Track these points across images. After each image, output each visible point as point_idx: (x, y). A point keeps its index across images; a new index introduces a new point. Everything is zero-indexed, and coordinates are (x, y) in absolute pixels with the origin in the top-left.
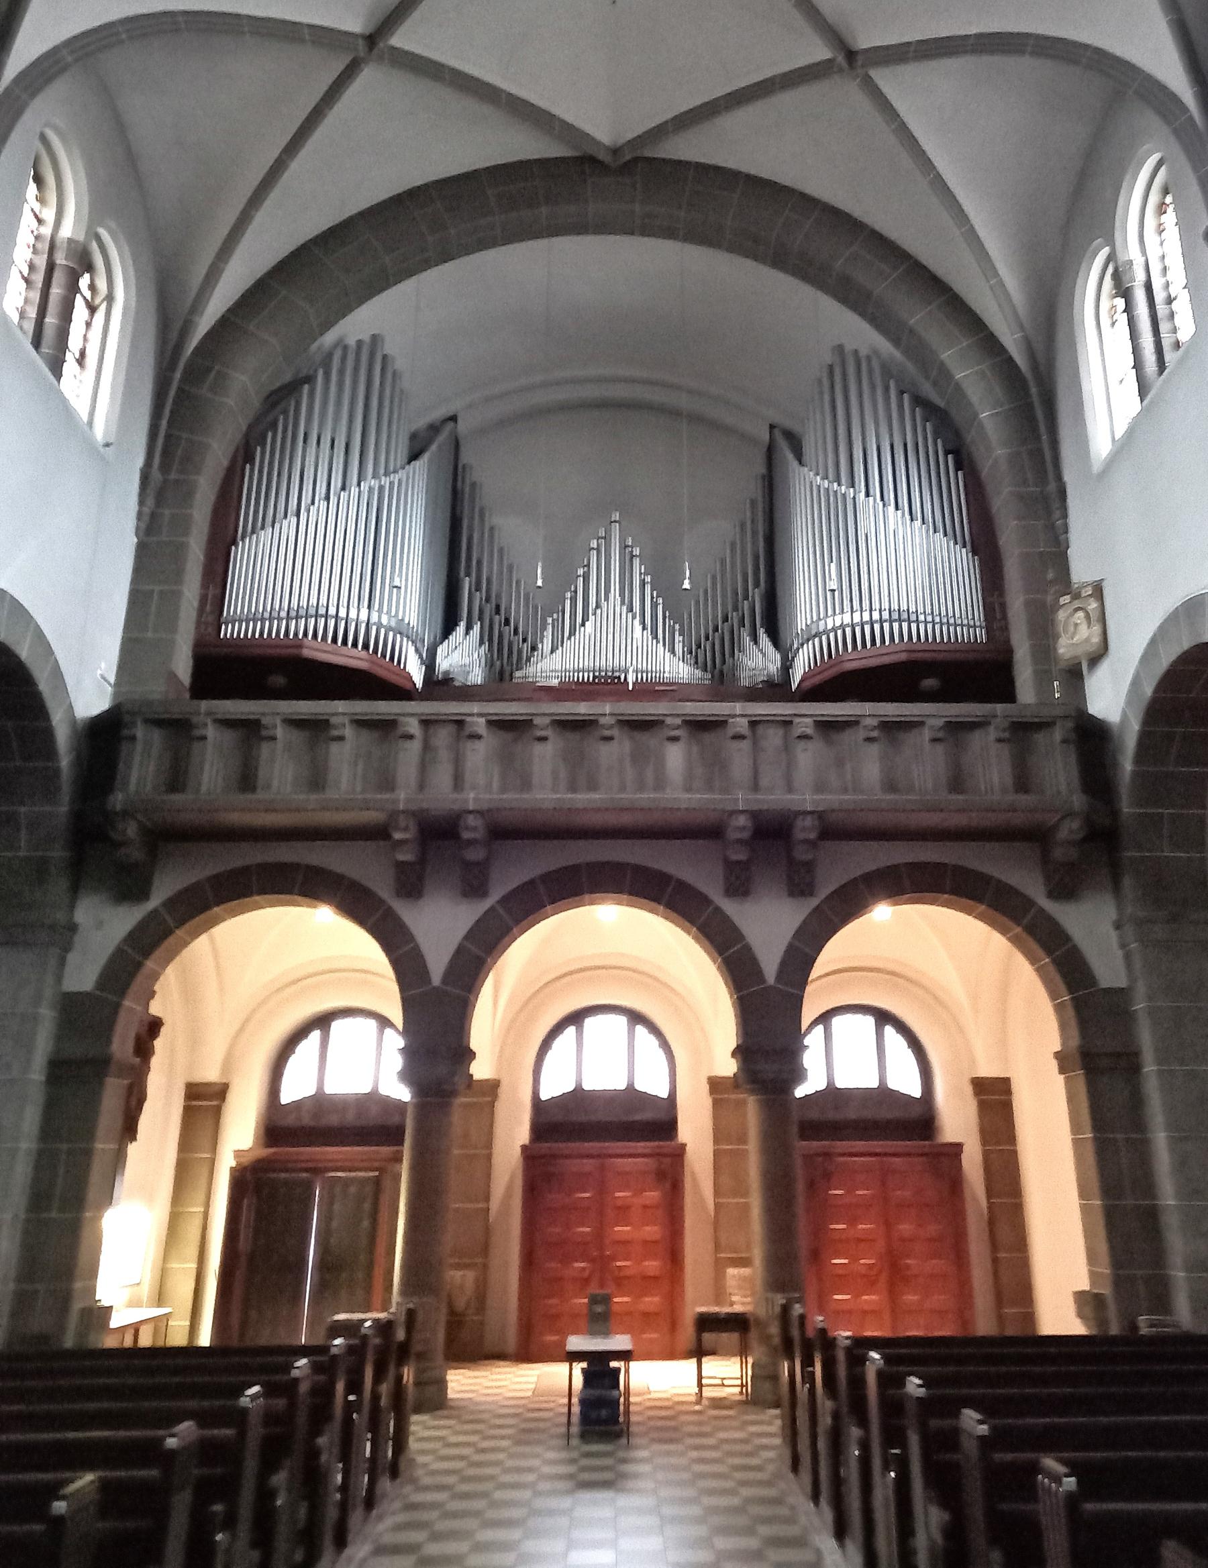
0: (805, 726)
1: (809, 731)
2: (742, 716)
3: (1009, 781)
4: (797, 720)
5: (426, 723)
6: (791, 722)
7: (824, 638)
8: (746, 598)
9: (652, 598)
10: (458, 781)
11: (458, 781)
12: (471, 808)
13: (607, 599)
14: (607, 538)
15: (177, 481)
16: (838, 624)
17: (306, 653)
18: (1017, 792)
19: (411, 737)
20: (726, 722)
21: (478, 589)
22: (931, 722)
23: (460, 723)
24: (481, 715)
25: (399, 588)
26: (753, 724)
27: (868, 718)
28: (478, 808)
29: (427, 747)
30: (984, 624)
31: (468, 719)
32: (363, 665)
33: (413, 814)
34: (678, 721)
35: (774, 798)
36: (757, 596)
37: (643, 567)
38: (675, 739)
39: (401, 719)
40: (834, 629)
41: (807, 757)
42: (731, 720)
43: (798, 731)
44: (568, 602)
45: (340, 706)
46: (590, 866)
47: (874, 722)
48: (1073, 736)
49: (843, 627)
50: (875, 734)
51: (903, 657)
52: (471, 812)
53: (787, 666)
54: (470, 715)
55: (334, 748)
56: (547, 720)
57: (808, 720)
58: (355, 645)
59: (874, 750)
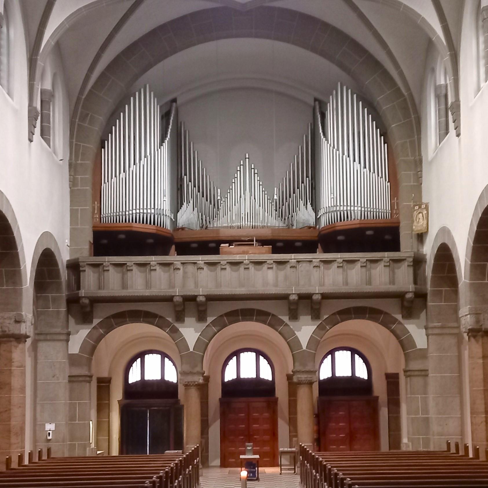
0: (316, 262)
1: (318, 264)
2: (294, 259)
3: (387, 280)
4: (314, 260)
5: (183, 264)
6: (312, 261)
7: (330, 214)
8: (303, 182)
9: (263, 191)
10: (196, 284)
11: (196, 284)
12: (201, 294)
13: (244, 193)
14: (244, 165)
15: (81, 164)
16: (335, 209)
17: (134, 229)
18: (390, 284)
19: (179, 269)
20: (288, 261)
21: (190, 181)
22: (361, 260)
23: (195, 263)
24: (202, 260)
25: (166, 201)
26: (298, 262)
27: (339, 259)
28: (203, 294)
29: (185, 273)
30: (390, 211)
31: (198, 262)
32: (154, 231)
33: (182, 296)
34: (272, 262)
35: (305, 290)
36: (307, 181)
37: (258, 178)
38: (272, 268)
39: (175, 262)
40: (332, 211)
41: (316, 274)
42: (290, 261)
43: (315, 264)
44: (229, 194)
45: (153, 258)
46: (242, 310)
47: (341, 260)
48: (412, 264)
49: (336, 211)
50: (341, 265)
51: (358, 226)
52: (201, 295)
53: (318, 220)
54: (199, 261)
55: (153, 273)
56: (225, 262)
57: (319, 260)
58: (150, 223)
59: (341, 270)
